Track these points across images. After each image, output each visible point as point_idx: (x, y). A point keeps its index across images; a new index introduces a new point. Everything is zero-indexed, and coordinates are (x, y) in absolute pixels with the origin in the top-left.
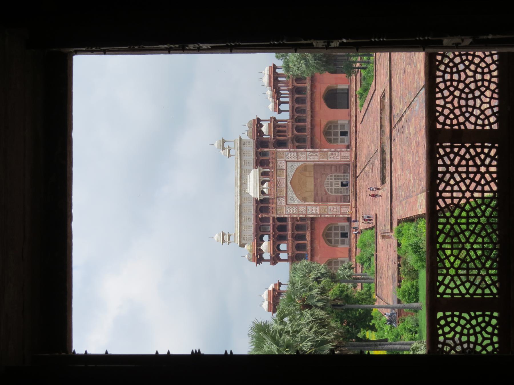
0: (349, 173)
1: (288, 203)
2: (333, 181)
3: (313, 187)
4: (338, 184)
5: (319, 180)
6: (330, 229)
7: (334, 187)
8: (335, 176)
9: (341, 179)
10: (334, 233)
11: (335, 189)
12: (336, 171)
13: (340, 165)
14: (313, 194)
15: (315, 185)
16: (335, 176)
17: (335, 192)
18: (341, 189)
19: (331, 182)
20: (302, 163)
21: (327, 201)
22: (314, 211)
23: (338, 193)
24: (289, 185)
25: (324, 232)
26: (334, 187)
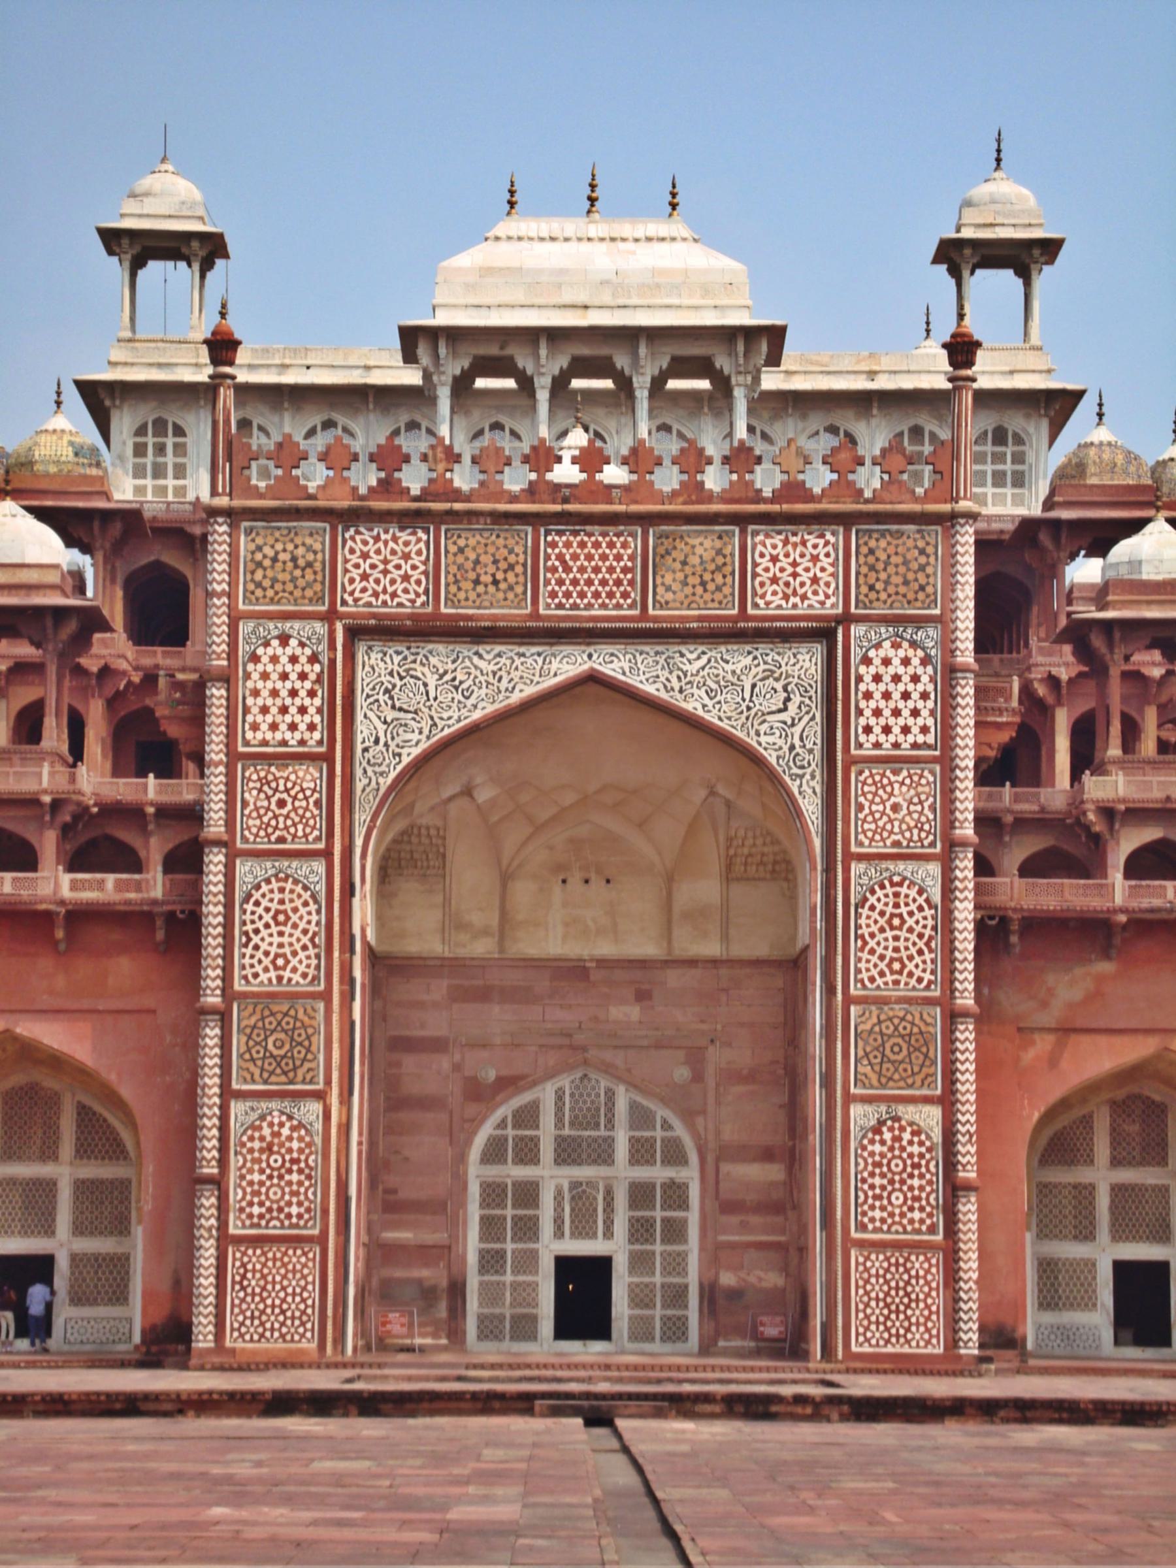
0: (706, 1348)
2: (623, 1171)
3: (552, 943)
4: (583, 1230)
5: (625, 1012)
6: (98, 1138)
7: (551, 1177)
8: (676, 1194)
9: (640, 1262)
10: (48, 1187)
11: (528, 1194)
12: (725, 1206)
13: (792, 1256)
14: (482, 948)
15: (574, 973)
16: (676, 1194)
17: (493, 1193)
18: (528, 1262)
19: (603, 1154)
20: (811, 808)
21: (393, 1105)
22: (268, 940)
23: (491, 1229)
24: (567, 664)
25: (56, 1062)
26: (551, 1177)
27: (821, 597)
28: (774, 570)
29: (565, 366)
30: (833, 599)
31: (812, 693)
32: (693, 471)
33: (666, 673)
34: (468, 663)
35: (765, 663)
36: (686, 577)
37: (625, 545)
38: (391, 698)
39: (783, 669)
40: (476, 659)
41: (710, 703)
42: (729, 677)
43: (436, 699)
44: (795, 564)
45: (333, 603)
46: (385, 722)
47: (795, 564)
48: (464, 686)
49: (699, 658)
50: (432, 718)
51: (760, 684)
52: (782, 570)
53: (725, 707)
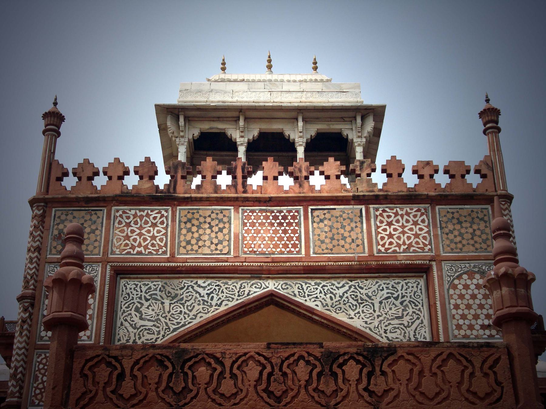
1: (129, 286)
27: (421, 246)
28: (390, 230)
29: (255, 135)
30: (429, 247)
31: (420, 306)
32: (333, 177)
33: (323, 296)
34: (191, 290)
35: (387, 288)
36: (333, 235)
37: (294, 217)
38: (140, 313)
39: (400, 292)
40: (196, 288)
41: (352, 313)
42: (365, 297)
43: (169, 312)
44: (403, 226)
45: (105, 252)
46: (135, 328)
47: (403, 226)
48: (188, 303)
49: (343, 286)
50: (166, 324)
51: (383, 301)
52: (395, 230)
53: (362, 315)
